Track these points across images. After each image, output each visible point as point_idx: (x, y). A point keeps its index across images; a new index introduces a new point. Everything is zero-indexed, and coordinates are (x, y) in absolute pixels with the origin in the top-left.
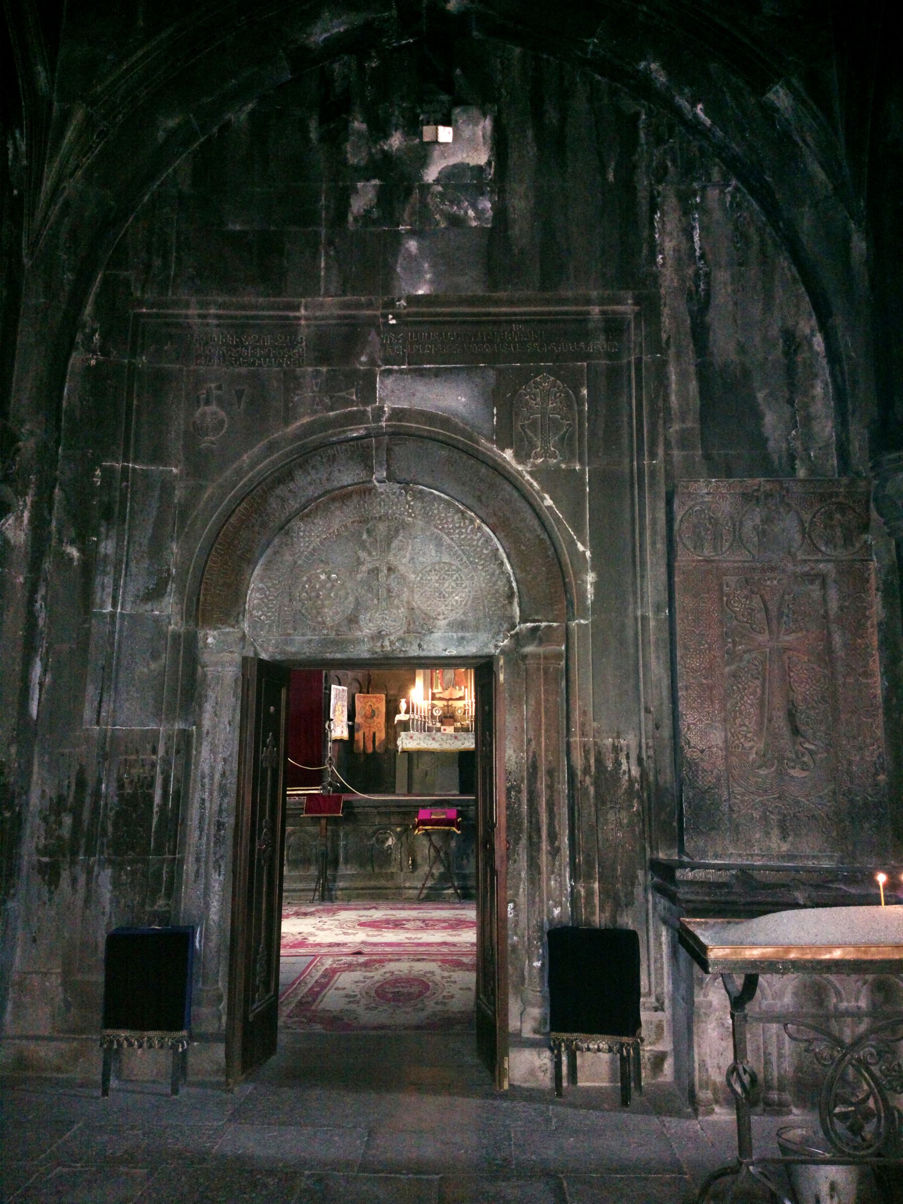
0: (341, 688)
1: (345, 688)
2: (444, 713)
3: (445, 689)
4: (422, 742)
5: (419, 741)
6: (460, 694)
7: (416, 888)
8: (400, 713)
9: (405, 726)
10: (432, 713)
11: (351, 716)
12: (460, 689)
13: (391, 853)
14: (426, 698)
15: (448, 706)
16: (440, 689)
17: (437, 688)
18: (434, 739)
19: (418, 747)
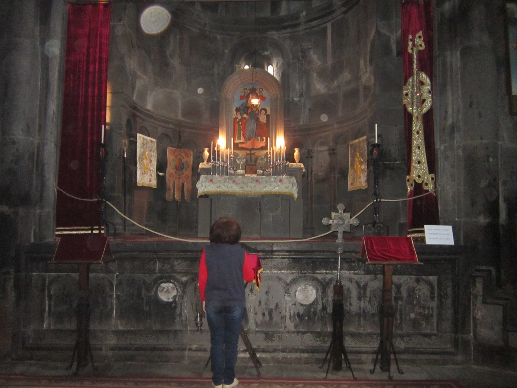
0: (149, 139)
1: (154, 140)
2: (247, 161)
3: (247, 139)
4: (222, 186)
5: (219, 184)
6: (263, 144)
7: (205, 350)
8: (203, 161)
9: (207, 171)
10: (235, 161)
11: (161, 167)
12: (262, 140)
13: (176, 307)
14: (228, 146)
15: (251, 154)
16: (242, 140)
17: (239, 138)
18: (234, 182)
19: (218, 190)
